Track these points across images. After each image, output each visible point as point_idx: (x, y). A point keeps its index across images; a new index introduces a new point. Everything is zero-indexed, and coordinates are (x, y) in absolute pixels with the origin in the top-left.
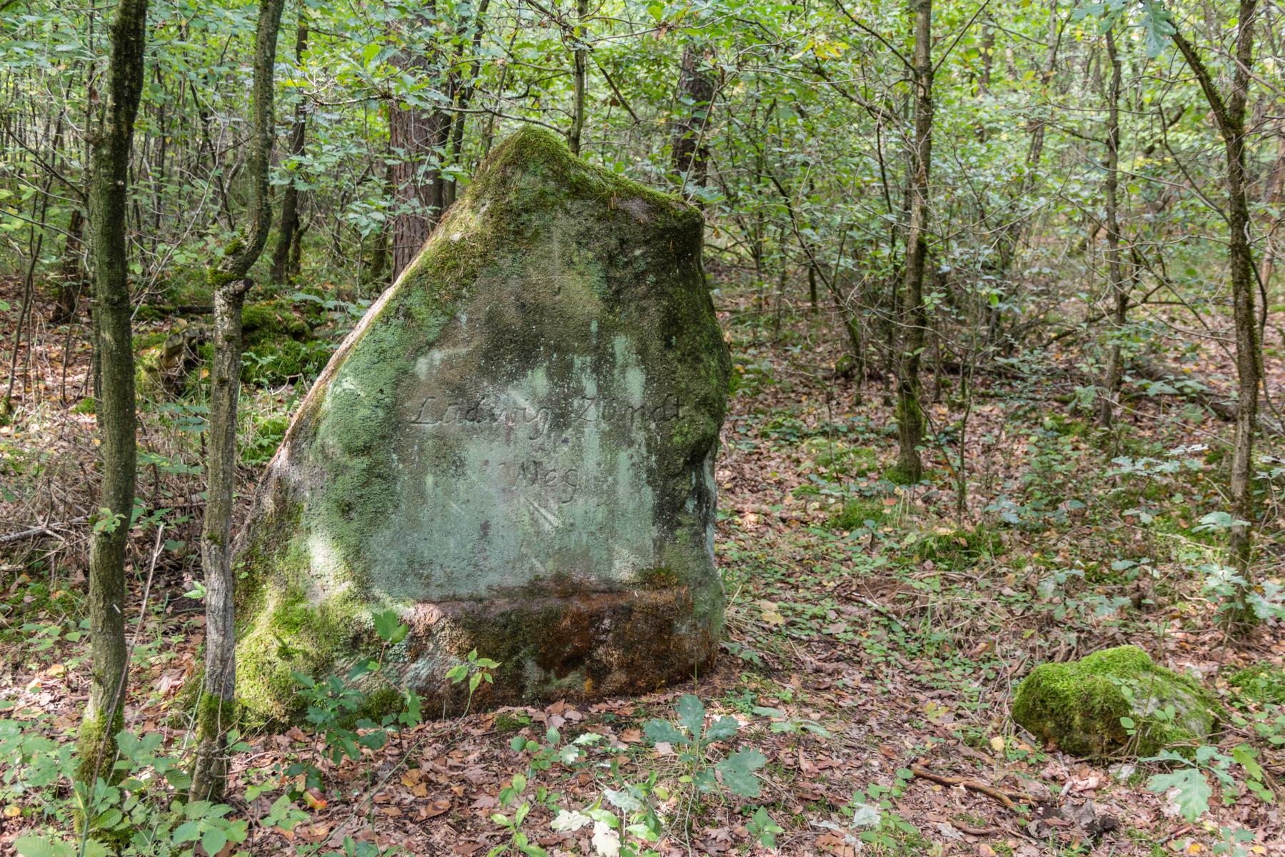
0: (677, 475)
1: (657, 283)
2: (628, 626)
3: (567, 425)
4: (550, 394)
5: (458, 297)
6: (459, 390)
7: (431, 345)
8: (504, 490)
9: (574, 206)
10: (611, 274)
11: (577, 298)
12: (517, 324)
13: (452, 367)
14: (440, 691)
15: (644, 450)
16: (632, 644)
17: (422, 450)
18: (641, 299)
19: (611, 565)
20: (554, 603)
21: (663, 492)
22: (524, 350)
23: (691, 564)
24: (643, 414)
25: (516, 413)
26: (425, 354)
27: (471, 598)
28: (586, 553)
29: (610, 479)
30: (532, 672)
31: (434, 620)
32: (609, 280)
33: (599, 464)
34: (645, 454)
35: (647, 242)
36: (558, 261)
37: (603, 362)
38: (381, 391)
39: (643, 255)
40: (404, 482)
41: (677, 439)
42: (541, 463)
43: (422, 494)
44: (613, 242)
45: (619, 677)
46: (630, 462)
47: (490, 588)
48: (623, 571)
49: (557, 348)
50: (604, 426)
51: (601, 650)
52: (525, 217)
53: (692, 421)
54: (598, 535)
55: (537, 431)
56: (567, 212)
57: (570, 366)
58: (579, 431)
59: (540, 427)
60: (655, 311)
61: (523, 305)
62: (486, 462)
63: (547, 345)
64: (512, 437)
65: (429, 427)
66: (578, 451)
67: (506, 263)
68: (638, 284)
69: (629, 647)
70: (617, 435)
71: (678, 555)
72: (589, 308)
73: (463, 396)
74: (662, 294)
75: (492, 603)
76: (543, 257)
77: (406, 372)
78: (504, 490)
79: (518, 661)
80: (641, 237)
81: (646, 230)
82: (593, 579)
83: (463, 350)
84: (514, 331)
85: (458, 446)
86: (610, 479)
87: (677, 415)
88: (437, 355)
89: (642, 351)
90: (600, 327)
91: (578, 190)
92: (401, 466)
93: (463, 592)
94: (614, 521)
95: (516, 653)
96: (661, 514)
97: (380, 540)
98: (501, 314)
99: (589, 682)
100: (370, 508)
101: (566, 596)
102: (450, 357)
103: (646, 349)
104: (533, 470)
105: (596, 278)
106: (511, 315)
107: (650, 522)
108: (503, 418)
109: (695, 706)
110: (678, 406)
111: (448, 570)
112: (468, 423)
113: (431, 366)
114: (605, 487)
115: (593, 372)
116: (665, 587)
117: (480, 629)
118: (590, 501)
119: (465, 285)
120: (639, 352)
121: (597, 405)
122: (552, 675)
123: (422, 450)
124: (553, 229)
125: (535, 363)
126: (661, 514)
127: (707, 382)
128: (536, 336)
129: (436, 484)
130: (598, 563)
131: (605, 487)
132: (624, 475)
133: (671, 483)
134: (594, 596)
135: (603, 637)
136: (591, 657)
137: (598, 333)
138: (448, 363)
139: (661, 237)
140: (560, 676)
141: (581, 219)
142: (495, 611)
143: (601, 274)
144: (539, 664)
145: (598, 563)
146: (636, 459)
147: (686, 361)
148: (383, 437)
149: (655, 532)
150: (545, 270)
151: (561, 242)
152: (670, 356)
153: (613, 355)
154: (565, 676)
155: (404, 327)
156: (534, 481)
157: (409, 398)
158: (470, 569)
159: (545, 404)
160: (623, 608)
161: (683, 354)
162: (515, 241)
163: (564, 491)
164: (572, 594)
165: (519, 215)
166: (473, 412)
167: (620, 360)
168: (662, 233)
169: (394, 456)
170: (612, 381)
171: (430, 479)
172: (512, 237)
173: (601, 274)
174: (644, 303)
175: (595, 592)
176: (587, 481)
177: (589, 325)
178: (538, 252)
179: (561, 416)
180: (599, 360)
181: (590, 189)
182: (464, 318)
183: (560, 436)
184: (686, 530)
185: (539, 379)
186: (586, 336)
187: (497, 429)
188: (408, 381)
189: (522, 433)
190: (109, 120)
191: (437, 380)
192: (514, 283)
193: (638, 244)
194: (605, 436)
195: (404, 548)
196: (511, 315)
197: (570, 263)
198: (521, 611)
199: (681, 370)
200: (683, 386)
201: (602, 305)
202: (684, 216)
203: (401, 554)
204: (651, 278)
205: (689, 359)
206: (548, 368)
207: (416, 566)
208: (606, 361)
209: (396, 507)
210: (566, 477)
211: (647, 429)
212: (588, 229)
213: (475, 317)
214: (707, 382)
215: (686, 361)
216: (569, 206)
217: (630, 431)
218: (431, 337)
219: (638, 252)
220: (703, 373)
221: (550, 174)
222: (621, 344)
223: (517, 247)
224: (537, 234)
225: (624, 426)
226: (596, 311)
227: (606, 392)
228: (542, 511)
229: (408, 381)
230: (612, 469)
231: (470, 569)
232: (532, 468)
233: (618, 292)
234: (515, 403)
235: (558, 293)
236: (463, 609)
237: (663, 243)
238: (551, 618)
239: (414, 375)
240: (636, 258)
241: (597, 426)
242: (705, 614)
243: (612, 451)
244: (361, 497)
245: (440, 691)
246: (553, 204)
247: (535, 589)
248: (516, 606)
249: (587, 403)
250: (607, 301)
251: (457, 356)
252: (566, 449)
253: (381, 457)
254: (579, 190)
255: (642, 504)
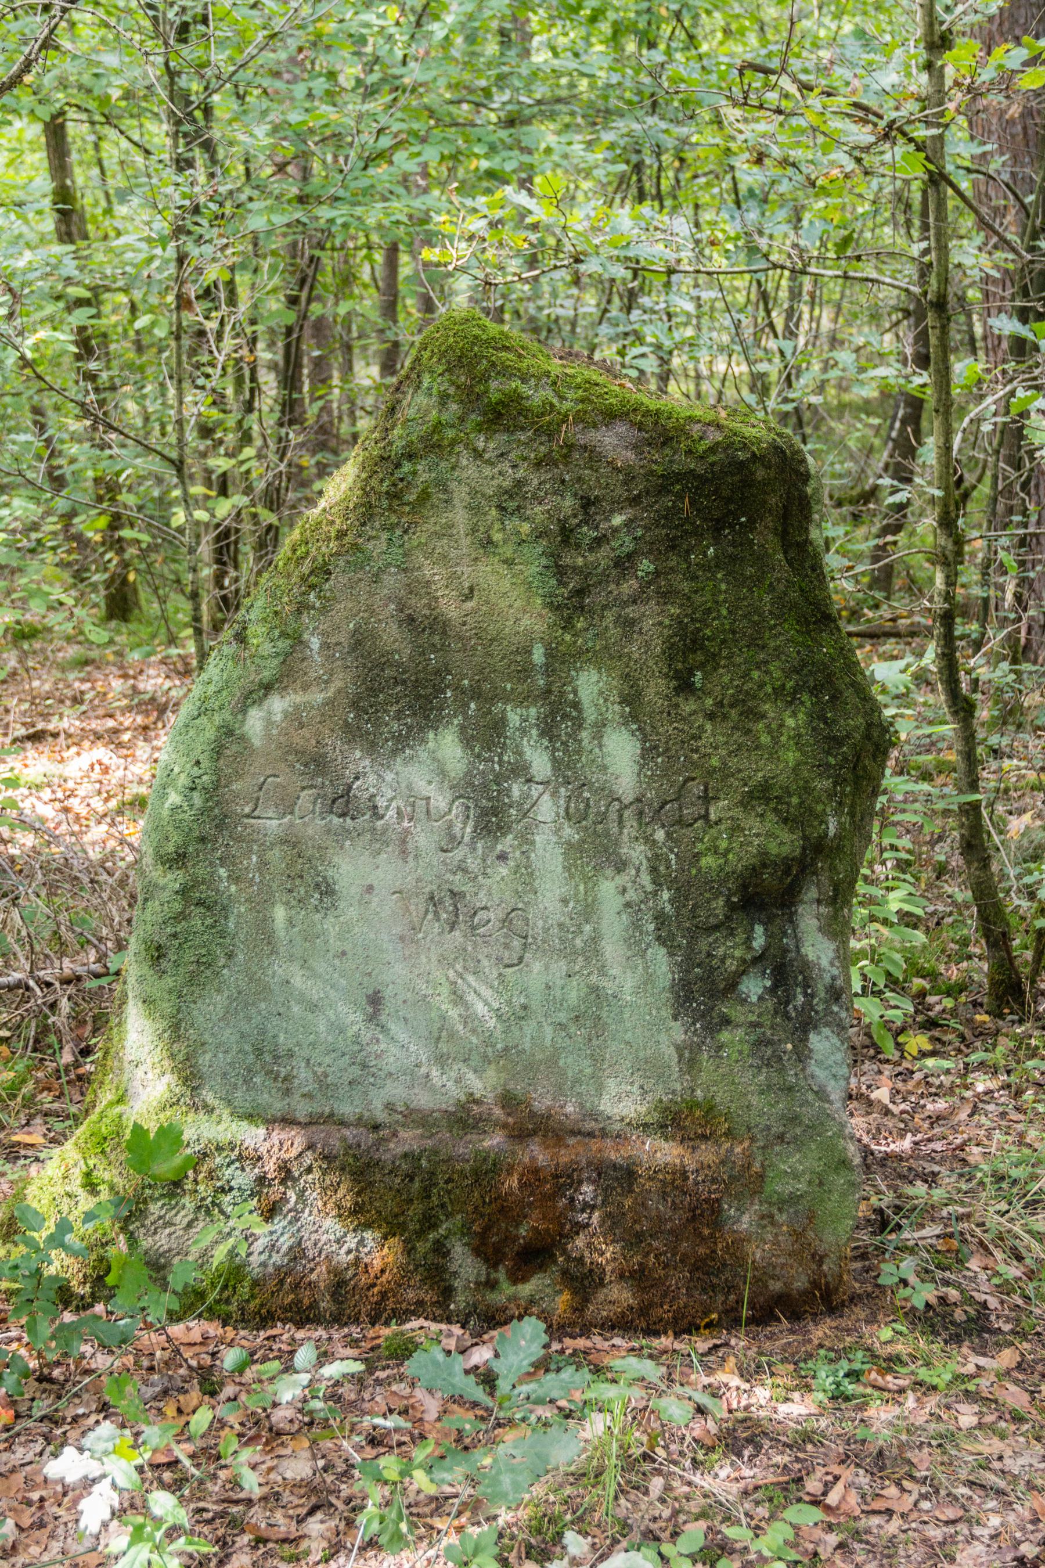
0: (716, 928)
1: (657, 573)
2: (628, 1202)
3: (503, 829)
4: (468, 773)
5: (302, 607)
6: (317, 763)
7: (267, 688)
8: (402, 938)
9: (490, 445)
10: (567, 560)
11: (503, 604)
12: (404, 653)
13: (302, 726)
14: (313, 1277)
15: (646, 879)
16: (639, 1237)
17: (263, 864)
18: (625, 604)
19: (600, 1089)
20: (493, 1141)
21: (688, 958)
22: (419, 697)
23: (754, 1100)
24: (641, 813)
25: (415, 807)
26: (259, 702)
27: (360, 1122)
28: (552, 1061)
29: (587, 928)
30: (465, 1266)
31: (294, 1152)
32: (560, 572)
33: (565, 901)
34: (650, 888)
35: (634, 501)
36: (465, 542)
37: (559, 717)
38: (198, 763)
39: (628, 524)
40: (239, 915)
41: (708, 861)
42: (462, 895)
43: (269, 938)
44: (569, 503)
45: (619, 1296)
46: (620, 901)
47: (390, 1107)
48: (622, 1101)
49: (476, 694)
50: (569, 832)
51: (580, 1241)
52: (407, 467)
53: (736, 829)
54: (573, 1029)
55: (452, 838)
56: (478, 454)
57: (499, 725)
58: (526, 839)
59: (457, 830)
60: (654, 620)
61: (411, 619)
62: (370, 888)
63: (457, 687)
64: (410, 846)
65: (272, 824)
66: (526, 876)
67: (377, 547)
68: (623, 577)
69: (634, 1240)
70: (594, 851)
71: (732, 1078)
72: (526, 622)
73: (324, 774)
74: (666, 596)
75: (395, 1134)
76: (439, 536)
77: (230, 733)
78: (402, 938)
79: (437, 1242)
80: (620, 492)
81: (629, 479)
82: (570, 1109)
83: (318, 697)
84: (399, 664)
85: (322, 859)
86: (587, 928)
87: (706, 817)
88: (277, 705)
89: (632, 700)
90: (550, 654)
91: (500, 415)
92: (233, 888)
93: (347, 1109)
94: (600, 1007)
95: (434, 1227)
96: (688, 999)
97: (211, 1005)
98: (374, 636)
99: (566, 1296)
100: (189, 956)
101: (520, 1134)
102: (297, 708)
103: (639, 695)
104: (450, 906)
105: (534, 569)
106: (392, 636)
107: (667, 1013)
108: (392, 813)
109: (532, 1340)
110: (707, 799)
111: (320, 1070)
112: (336, 820)
113: (269, 722)
114: (578, 942)
115: (542, 734)
116: (704, 1137)
117: (387, 1181)
118: (554, 967)
119: (312, 587)
120: (625, 700)
121: (555, 794)
122: (501, 1275)
123: (263, 864)
124: (453, 485)
125: (439, 719)
126: (688, 999)
127: (773, 755)
128: (437, 672)
129: (291, 923)
130: (576, 1081)
131: (578, 942)
132: (612, 923)
133: (703, 944)
134: (571, 1141)
135: (582, 1217)
136: (564, 1252)
137: (547, 665)
138: (296, 718)
139: (663, 490)
140: (517, 1277)
141: (505, 466)
142: (396, 1148)
143: (544, 561)
144: (477, 1252)
145: (576, 1081)
146: (632, 895)
147: (725, 717)
148: (203, 840)
149: (678, 1032)
150: (444, 557)
151: (469, 508)
152: (688, 706)
153: (576, 705)
154: (524, 1280)
155: (236, 659)
156: (453, 927)
157: (239, 775)
158: (355, 1071)
159: (466, 789)
160: (615, 1167)
161: (720, 704)
162: (390, 509)
163: (507, 946)
164: (534, 1133)
165: (398, 466)
166: (342, 802)
167: (590, 715)
168: (665, 483)
169: (222, 872)
170: (579, 752)
171: (280, 913)
172: (385, 503)
173: (544, 561)
174: (631, 611)
175: (574, 1133)
176: (546, 930)
177: (529, 652)
178: (429, 527)
179: (492, 817)
180: (553, 713)
181: (523, 412)
182: (315, 643)
183: (492, 848)
184: (740, 1033)
185: (447, 746)
186: (525, 671)
187: (385, 831)
188: (235, 748)
189: (424, 839)
190: (273, 366)
191: (279, 746)
192: (392, 581)
193: (618, 505)
194: (571, 849)
195: (245, 1027)
196: (392, 636)
197: (488, 543)
198: (436, 1153)
199: (711, 733)
200: (715, 762)
201: (551, 617)
202: (712, 449)
203: (242, 1036)
204: (646, 565)
205: (734, 713)
206: (463, 728)
207: (268, 1058)
208: (565, 716)
209: (230, 956)
210: (506, 921)
211: (652, 843)
212: (519, 483)
213: (333, 640)
214: (773, 755)
215: (725, 717)
216: (481, 445)
217: (617, 843)
218: (266, 675)
219: (618, 520)
220: (765, 739)
221: (452, 391)
222: (590, 685)
223: (394, 519)
224: (424, 497)
225: (607, 834)
226: (540, 627)
227: (567, 771)
228: (471, 979)
229: (235, 748)
230: (588, 911)
231: (355, 1071)
232: (448, 901)
233: (580, 593)
234: (410, 787)
235: (469, 597)
236: (344, 1139)
237: (668, 501)
238: (486, 1171)
239: (243, 738)
240: (615, 530)
241: (557, 831)
242: (794, 1199)
243: (586, 880)
244: (175, 936)
245: (313, 1277)
246: (453, 443)
247: (465, 1118)
248: (429, 1143)
249: (536, 790)
250: (558, 608)
251: (308, 706)
252: (504, 871)
253: (201, 871)
254: (502, 415)
255: (649, 979)
